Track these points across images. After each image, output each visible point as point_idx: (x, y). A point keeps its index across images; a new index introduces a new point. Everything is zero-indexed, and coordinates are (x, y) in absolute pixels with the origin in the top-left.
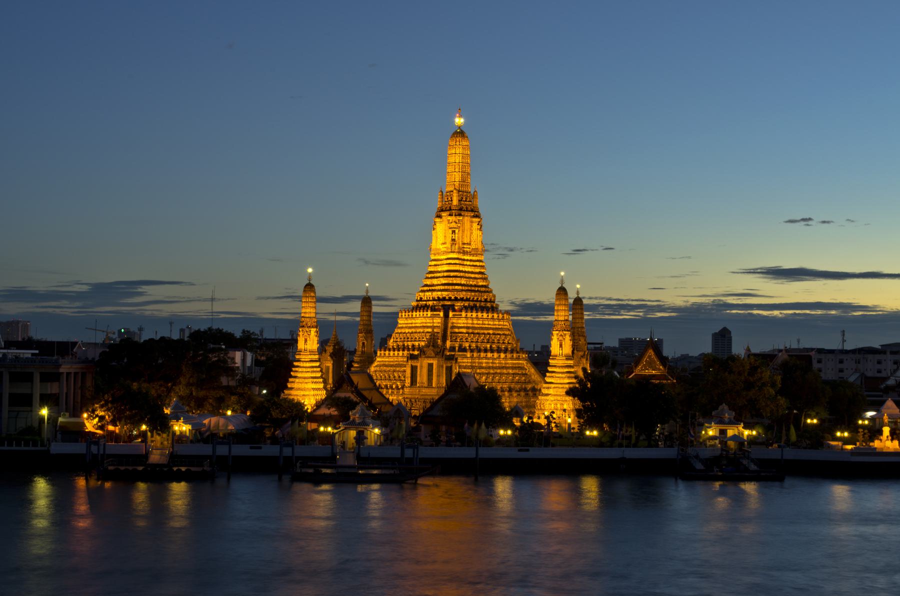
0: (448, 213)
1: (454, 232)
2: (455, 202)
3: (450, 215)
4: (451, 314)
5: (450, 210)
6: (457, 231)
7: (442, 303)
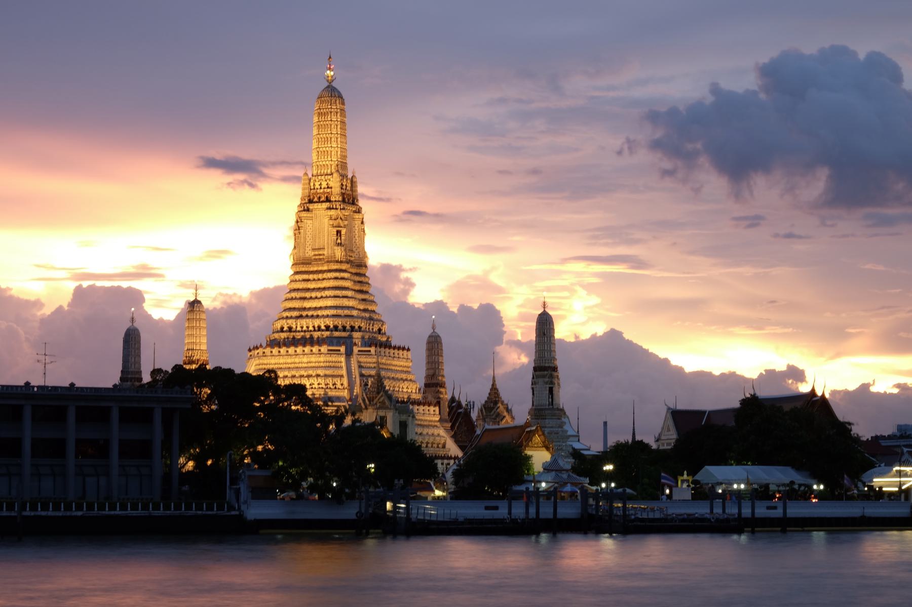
0: (325, 205)
1: (339, 232)
2: (336, 190)
3: (329, 208)
4: (356, 349)
5: (328, 200)
6: (343, 231)
7: (336, 334)
